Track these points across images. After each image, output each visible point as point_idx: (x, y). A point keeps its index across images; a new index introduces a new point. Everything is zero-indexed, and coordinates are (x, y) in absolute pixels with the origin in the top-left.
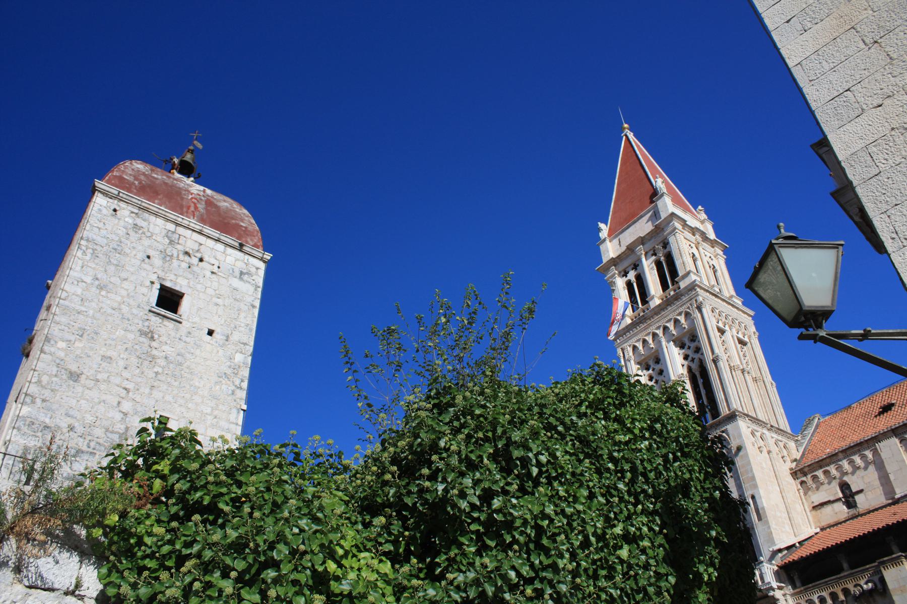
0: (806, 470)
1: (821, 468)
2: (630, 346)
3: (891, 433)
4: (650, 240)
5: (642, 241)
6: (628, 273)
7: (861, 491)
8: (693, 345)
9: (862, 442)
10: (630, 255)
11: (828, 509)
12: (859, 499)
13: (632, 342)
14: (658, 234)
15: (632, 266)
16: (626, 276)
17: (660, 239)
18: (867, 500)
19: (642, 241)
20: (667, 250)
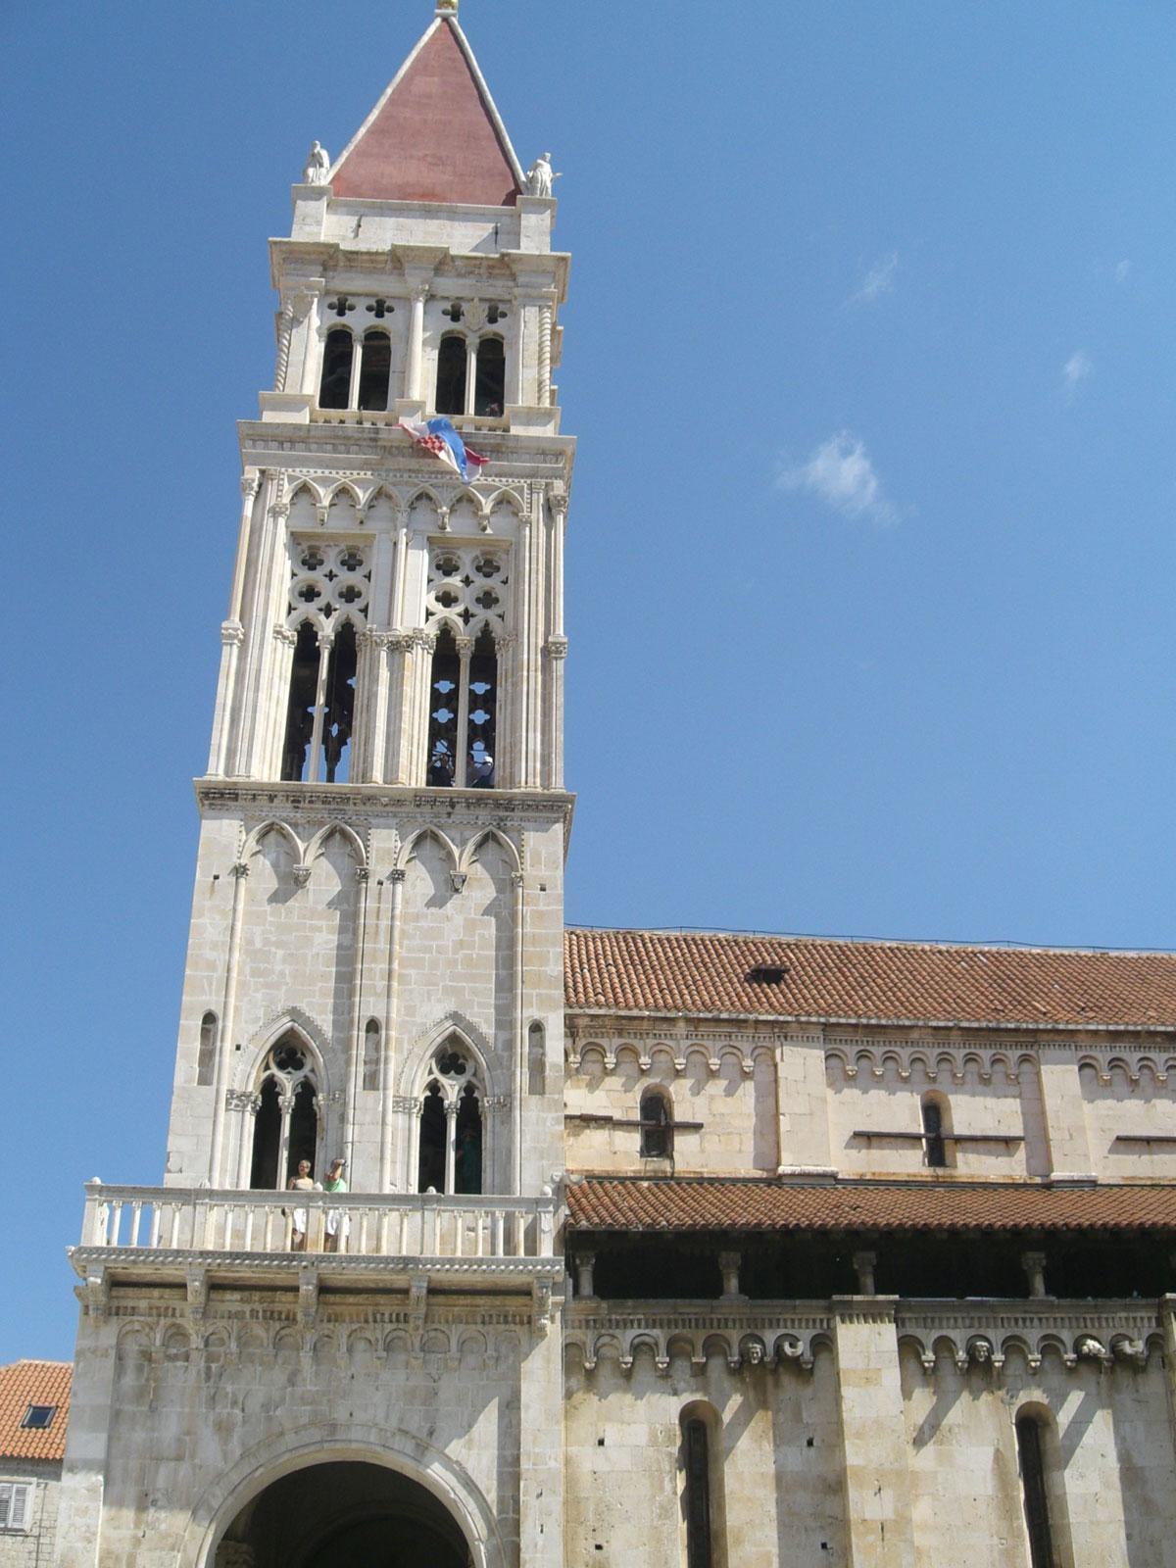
0: (582, 1022)
1: (620, 1033)
2: (291, 479)
3: (818, 1033)
4: (459, 275)
5: (441, 263)
6: (352, 308)
7: (696, 1127)
8: (481, 582)
9: (745, 1021)
10: (382, 271)
11: (597, 1137)
12: (682, 1143)
13: (307, 474)
14: (490, 276)
15: (373, 302)
16: (341, 313)
17: (497, 289)
18: (703, 1151)
19: (441, 262)
20: (500, 327)
